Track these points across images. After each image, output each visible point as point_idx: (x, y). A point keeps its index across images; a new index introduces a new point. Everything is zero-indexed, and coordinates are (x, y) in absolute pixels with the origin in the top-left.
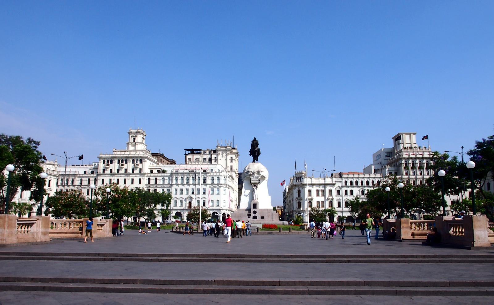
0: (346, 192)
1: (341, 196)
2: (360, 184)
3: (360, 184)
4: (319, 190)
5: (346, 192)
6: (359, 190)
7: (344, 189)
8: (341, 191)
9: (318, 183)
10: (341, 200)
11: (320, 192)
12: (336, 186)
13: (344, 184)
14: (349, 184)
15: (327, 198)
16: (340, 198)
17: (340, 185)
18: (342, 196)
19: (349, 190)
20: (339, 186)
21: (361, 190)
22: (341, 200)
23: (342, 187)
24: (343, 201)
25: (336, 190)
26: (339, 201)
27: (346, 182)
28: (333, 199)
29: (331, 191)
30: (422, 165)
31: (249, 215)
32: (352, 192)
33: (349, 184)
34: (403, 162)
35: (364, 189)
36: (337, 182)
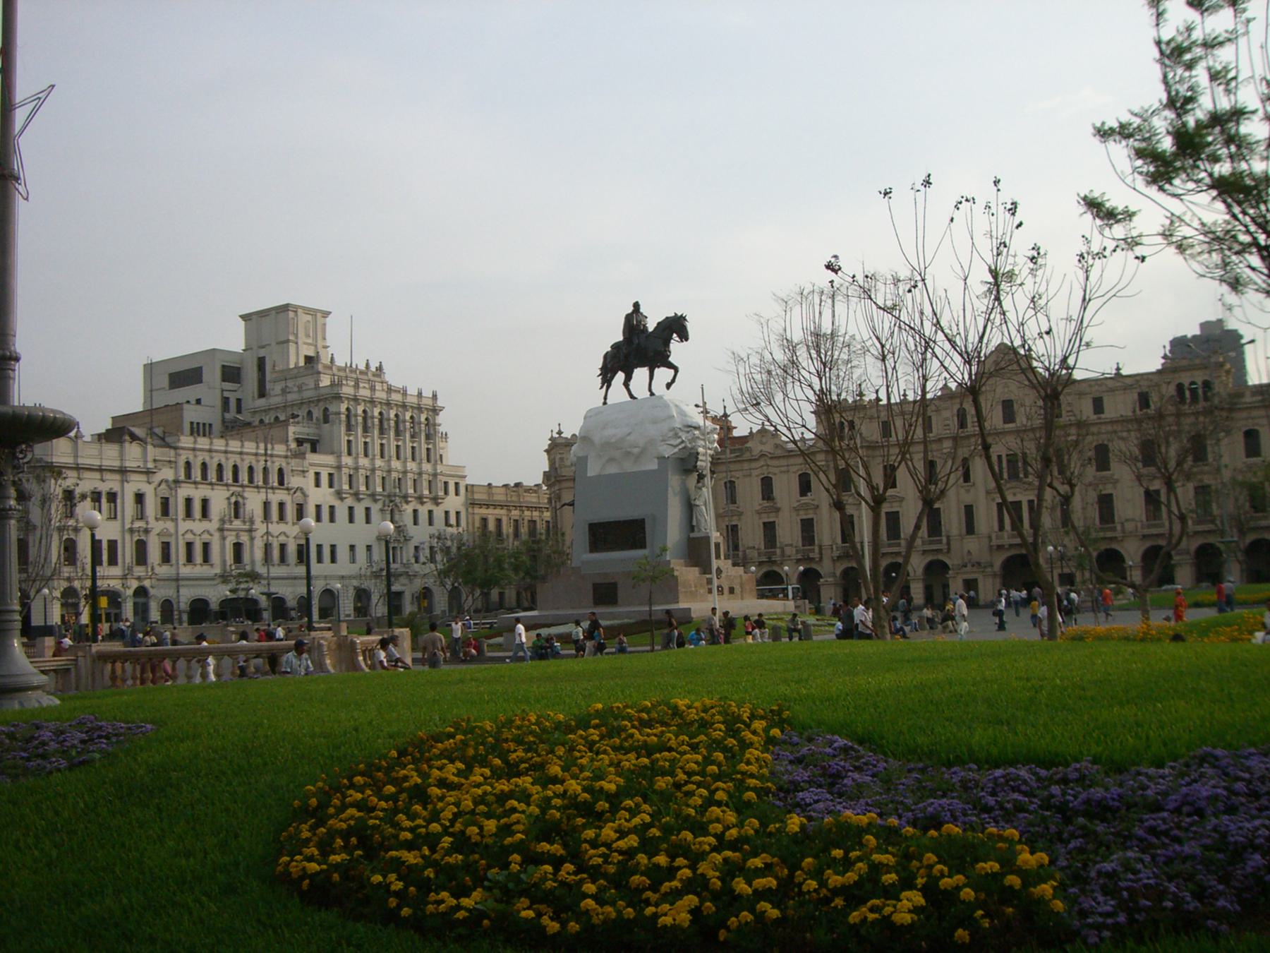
0: (189, 501)
1: (172, 520)
2: (228, 476)
3: (228, 476)
4: (99, 494)
5: (189, 501)
6: (228, 499)
7: (184, 491)
8: (171, 501)
9: (97, 462)
10: (174, 537)
11: (104, 500)
12: (157, 478)
13: (182, 477)
14: (197, 474)
15: (128, 526)
16: (169, 525)
17: (167, 474)
18: (175, 520)
19: (197, 494)
20: (167, 481)
21: (233, 500)
22: (171, 535)
23: (176, 482)
24: (180, 538)
25: (156, 495)
26: (166, 540)
27: (188, 465)
28: (147, 531)
29: (139, 498)
30: (432, 432)
31: (710, 581)
32: (205, 502)
33: (197, 474)
34: (343, 407)
35: (244, 498)
36: (159, 464)
